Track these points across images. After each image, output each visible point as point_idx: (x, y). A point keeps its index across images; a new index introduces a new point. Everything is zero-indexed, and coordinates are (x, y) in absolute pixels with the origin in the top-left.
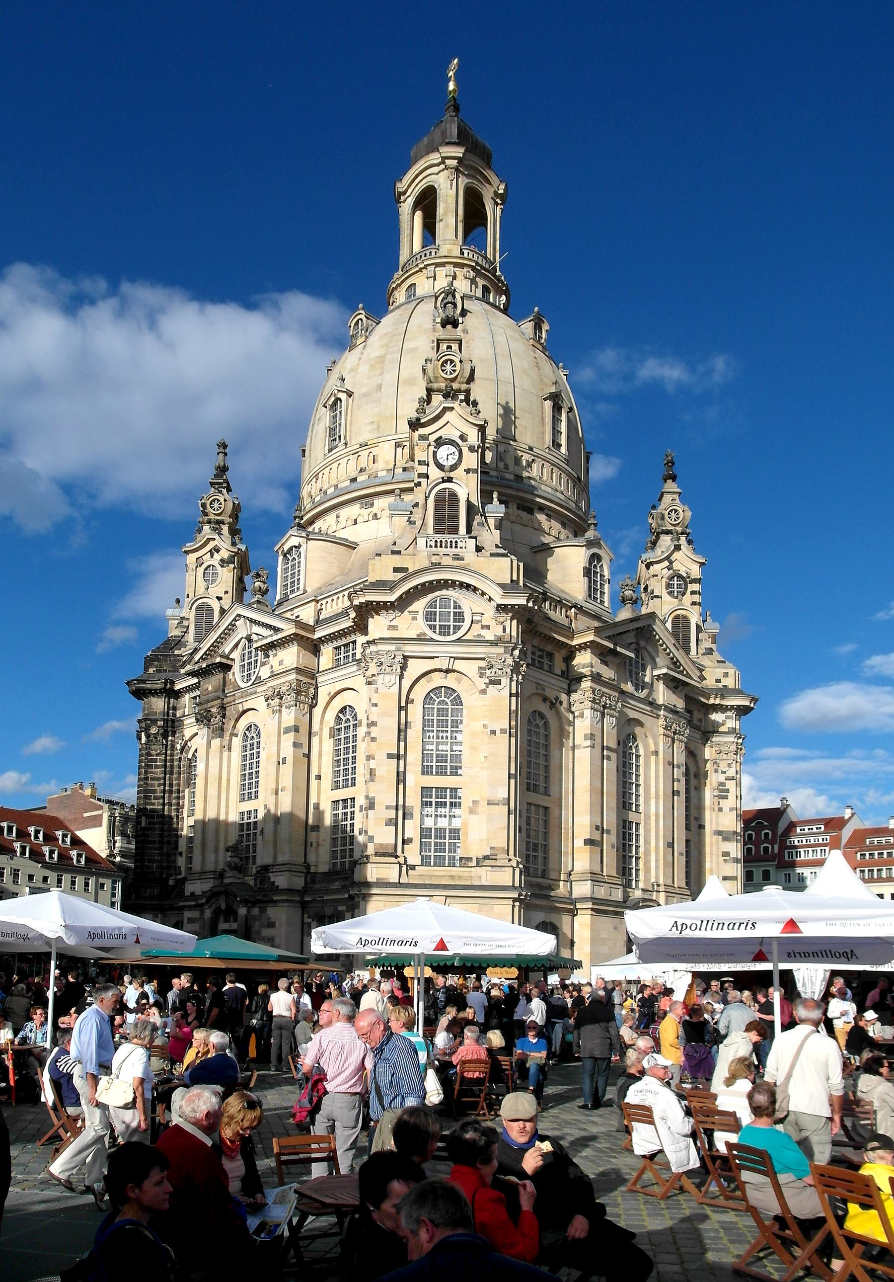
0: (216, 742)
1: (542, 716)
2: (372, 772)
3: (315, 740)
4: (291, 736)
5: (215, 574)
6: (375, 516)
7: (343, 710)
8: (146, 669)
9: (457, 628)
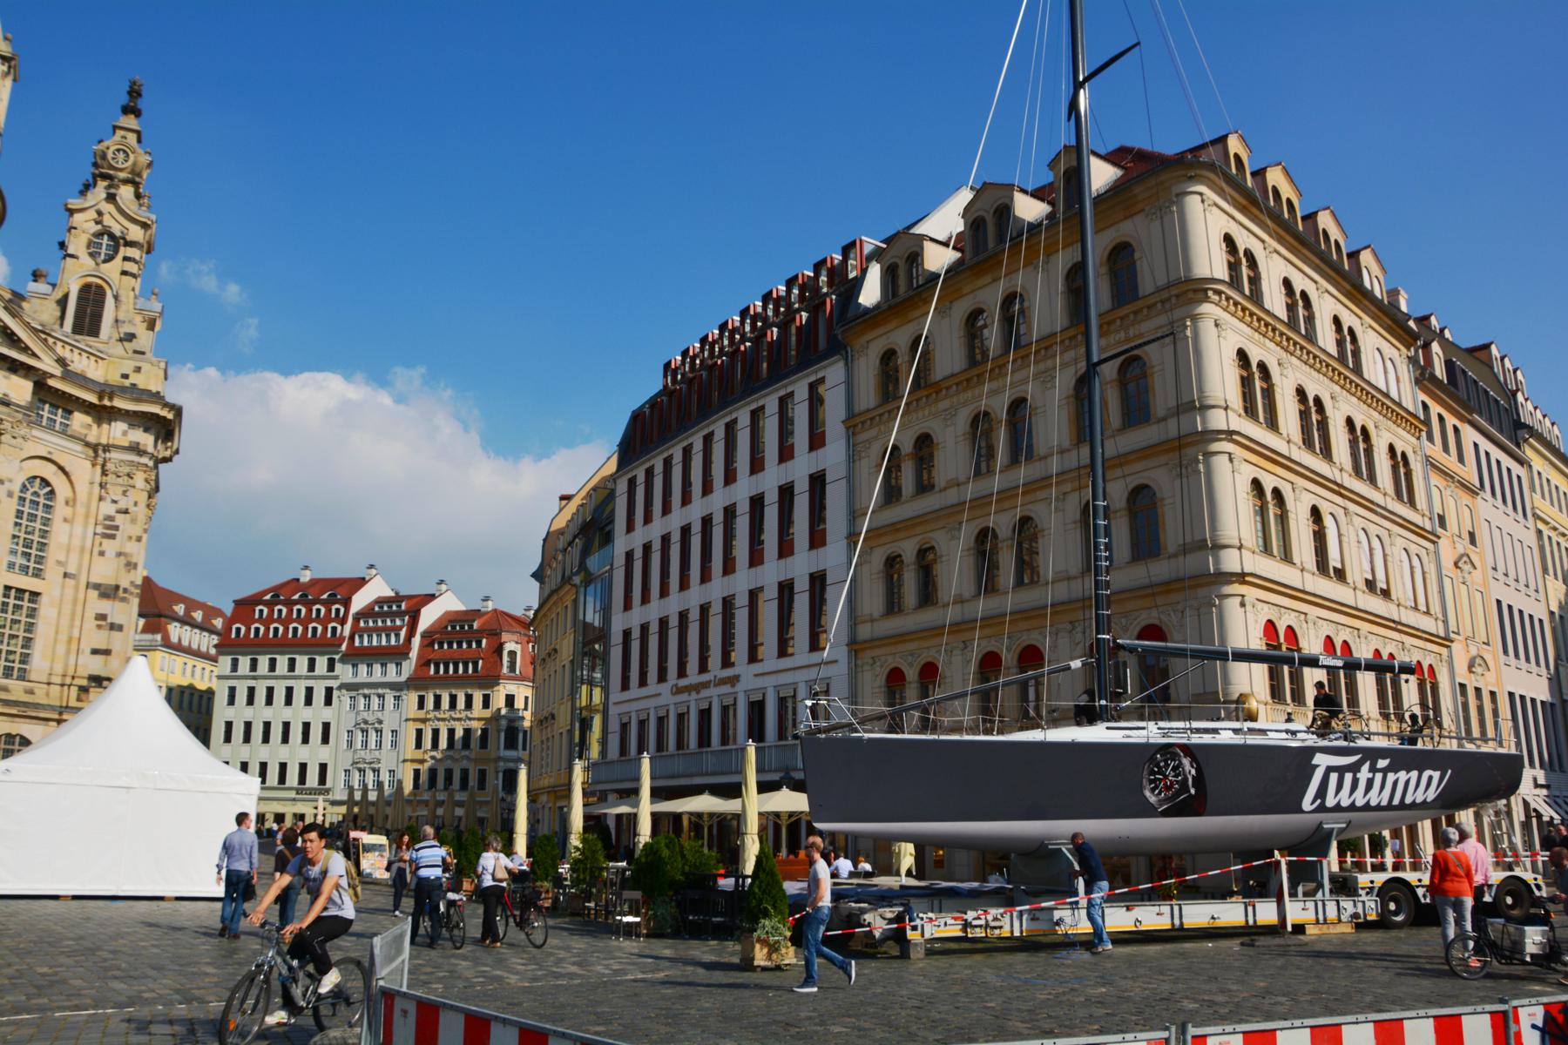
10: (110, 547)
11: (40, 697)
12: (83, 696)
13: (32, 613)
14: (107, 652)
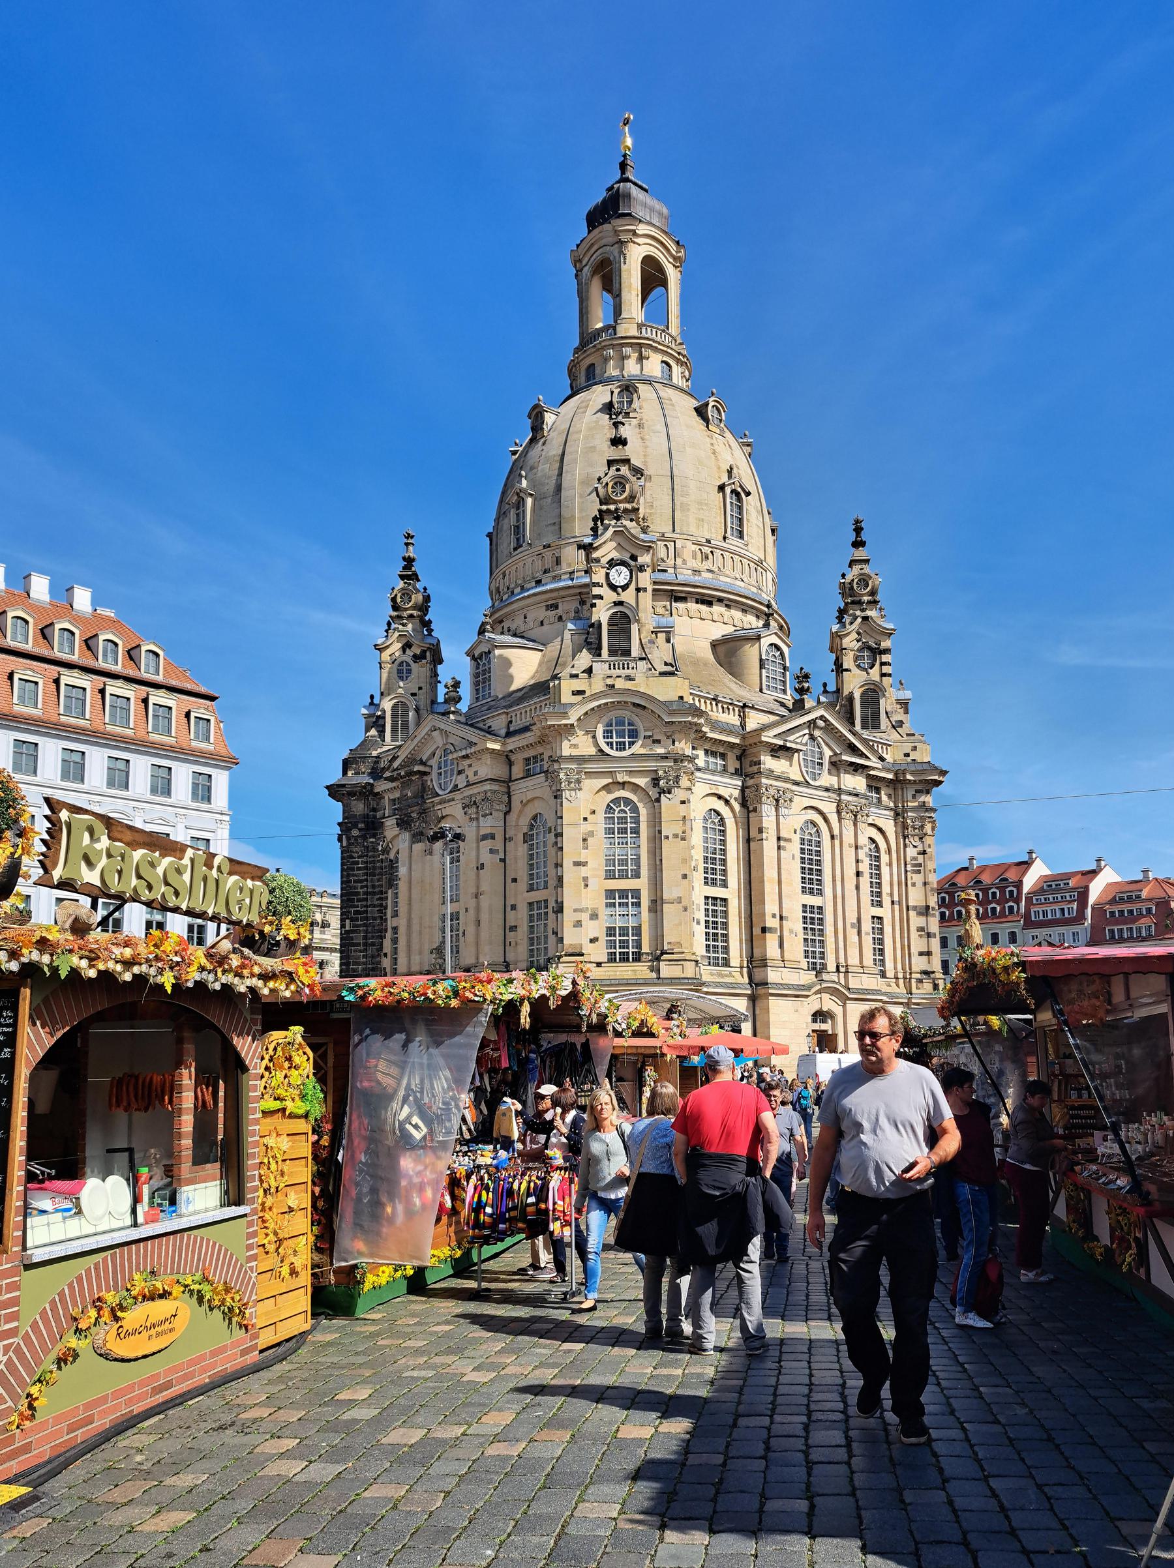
0: (419, 847)
1: (718, 814)
2: (560, 879)
3: (510, 845)
4: (487, 845)
5: (409, 671)
6: (560, 618)
7: (535, 818)
8: (345, 773)
9: (632, 744)
10: (918, 879)
12: (920, 985)
14: (929, 953)
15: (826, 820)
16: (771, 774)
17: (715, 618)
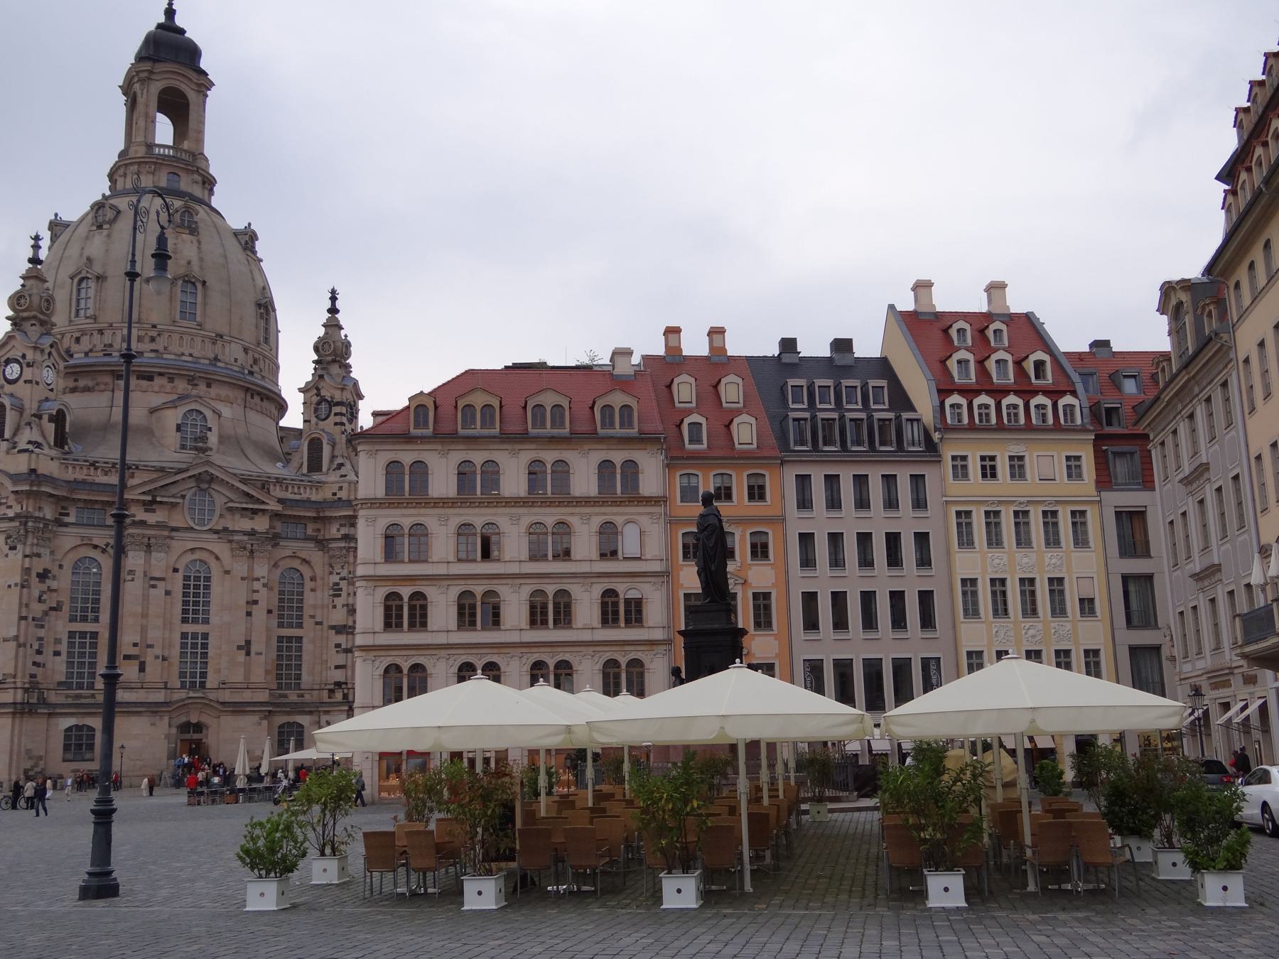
10: (339, 602)
11: (307, 697)
13: (300, 649)
14: (343, 667)
15: (217, 558)
16: (143, 523)
17: (156, 389)
